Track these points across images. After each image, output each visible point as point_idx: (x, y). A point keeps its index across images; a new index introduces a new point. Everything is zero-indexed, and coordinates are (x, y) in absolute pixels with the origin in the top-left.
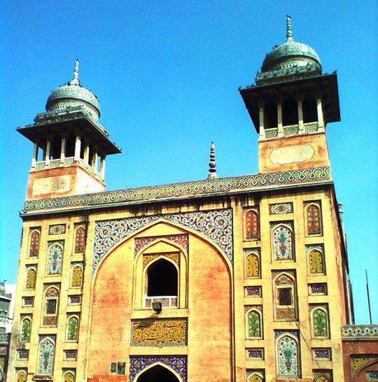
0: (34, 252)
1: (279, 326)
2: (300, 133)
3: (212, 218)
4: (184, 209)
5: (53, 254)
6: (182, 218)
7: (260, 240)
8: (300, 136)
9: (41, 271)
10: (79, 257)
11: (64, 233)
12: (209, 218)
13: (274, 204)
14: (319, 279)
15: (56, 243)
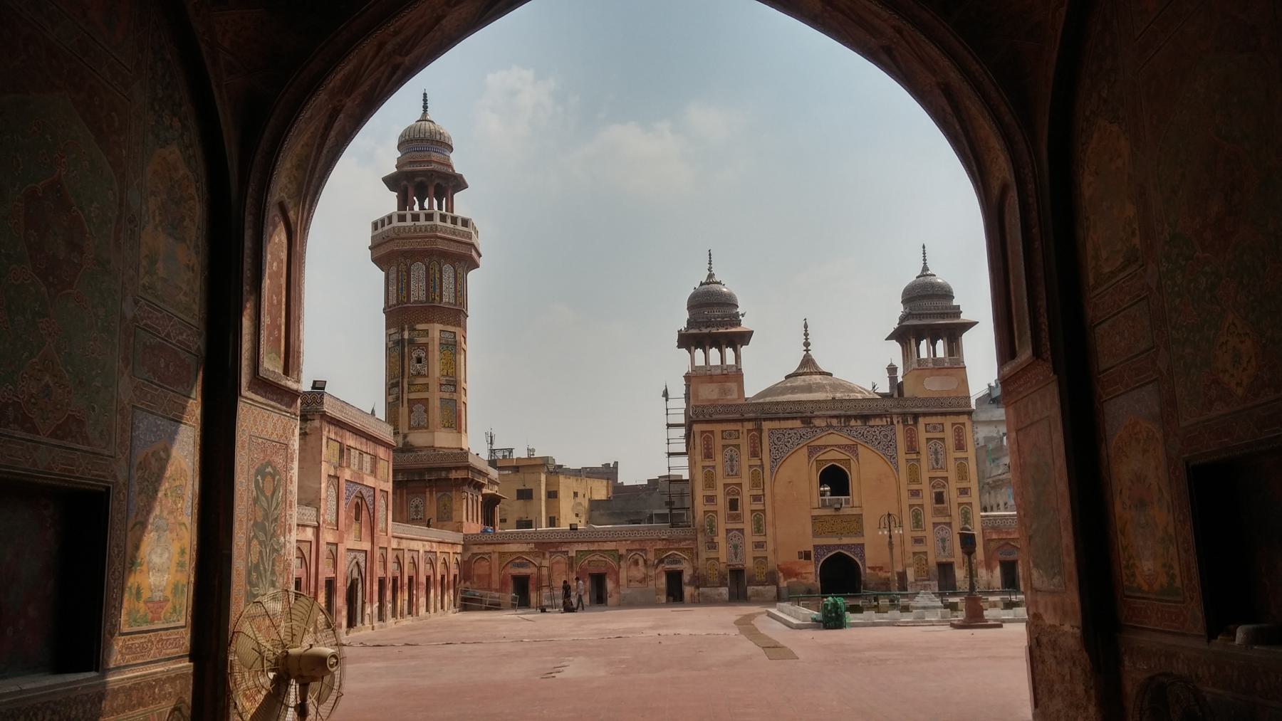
0: (708, 455)
1: (937, 520)
2: (946, 364)
3: (878, 432)
4: (853, 423)
5: (728, 457)
6: (851, 431)
7: (919, 453)
8: (946, 368)
9: (719, 470)
10: (756, 462)
11: (739, 438)
12: (875, 432)
13: (929, 424)
14: (964, 485)
15: (731, 447)
